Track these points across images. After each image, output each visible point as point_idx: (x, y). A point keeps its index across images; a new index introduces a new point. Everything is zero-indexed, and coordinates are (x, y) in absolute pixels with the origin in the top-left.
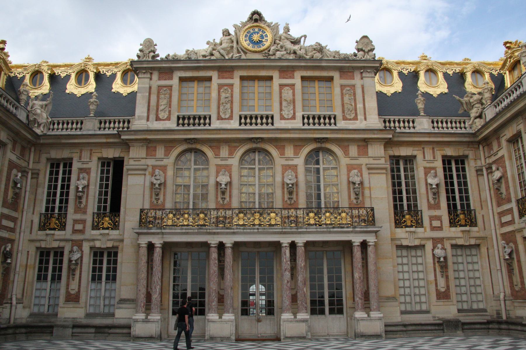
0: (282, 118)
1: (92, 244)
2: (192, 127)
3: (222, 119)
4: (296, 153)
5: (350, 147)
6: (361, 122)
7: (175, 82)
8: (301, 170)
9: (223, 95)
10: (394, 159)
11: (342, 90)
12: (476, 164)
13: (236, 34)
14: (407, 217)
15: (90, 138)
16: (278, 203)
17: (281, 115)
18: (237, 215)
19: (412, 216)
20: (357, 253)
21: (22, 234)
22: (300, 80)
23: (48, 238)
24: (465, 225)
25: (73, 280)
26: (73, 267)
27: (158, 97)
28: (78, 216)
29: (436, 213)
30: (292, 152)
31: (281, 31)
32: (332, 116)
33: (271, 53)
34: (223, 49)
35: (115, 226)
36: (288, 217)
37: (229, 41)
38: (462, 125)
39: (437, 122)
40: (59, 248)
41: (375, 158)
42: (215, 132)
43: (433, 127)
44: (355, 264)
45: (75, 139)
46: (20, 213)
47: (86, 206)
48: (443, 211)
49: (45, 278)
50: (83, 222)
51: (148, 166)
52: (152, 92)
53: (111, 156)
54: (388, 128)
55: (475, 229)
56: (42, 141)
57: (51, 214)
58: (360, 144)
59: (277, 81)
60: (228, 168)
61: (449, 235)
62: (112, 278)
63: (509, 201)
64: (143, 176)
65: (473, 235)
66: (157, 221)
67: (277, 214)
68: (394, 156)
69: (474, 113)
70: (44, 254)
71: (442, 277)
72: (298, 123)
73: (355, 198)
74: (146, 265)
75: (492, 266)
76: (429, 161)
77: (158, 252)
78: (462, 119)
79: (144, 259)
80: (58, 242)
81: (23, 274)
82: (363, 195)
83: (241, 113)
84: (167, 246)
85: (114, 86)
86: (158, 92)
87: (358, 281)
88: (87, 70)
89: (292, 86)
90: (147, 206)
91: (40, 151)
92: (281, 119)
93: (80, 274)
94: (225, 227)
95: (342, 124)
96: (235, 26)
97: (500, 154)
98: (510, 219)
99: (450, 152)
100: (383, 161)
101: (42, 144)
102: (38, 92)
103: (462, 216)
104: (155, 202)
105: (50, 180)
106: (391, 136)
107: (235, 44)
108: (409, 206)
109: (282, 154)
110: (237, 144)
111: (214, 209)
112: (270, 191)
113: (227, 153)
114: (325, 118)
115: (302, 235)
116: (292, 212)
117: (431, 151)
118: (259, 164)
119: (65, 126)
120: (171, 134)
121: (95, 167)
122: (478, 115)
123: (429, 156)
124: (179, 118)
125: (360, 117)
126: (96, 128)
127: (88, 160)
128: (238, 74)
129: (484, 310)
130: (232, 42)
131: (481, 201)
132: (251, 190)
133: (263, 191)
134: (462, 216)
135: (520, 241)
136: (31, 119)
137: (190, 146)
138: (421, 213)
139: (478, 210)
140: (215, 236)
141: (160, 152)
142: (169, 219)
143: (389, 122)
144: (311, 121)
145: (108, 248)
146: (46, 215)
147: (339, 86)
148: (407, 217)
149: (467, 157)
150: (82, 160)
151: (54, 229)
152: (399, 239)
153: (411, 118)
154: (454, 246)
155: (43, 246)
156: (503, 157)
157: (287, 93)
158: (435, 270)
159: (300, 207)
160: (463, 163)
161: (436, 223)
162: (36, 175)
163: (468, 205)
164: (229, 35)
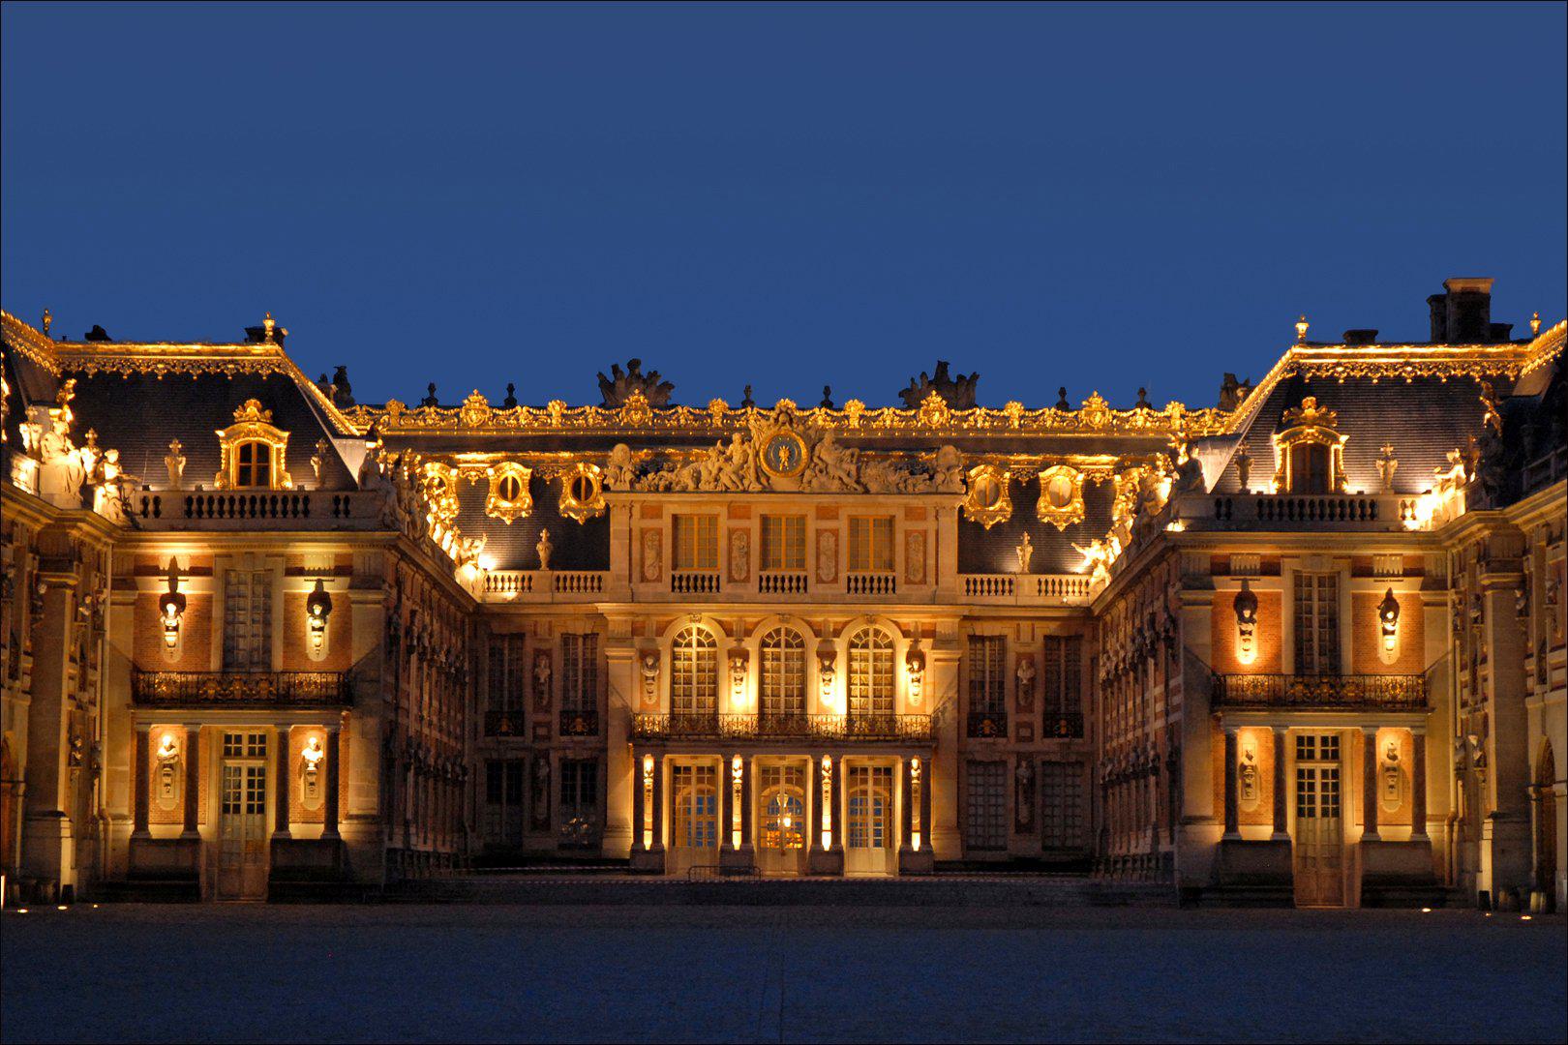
0: (820, 581)
1: (561, 754)
9: (736, 543)
27: (642, 544)
28: (541, 717)
29: (1025, 718)
47: (550, 703)
48: (1037, 720)
49: (499, 801)
50: (548, 725)
70: (493, 767)
125: (931, 579)
151: (507, 734)
154: (1044, 763)
155: (495, 756)
157: (828, 542)
162: (475, 661)
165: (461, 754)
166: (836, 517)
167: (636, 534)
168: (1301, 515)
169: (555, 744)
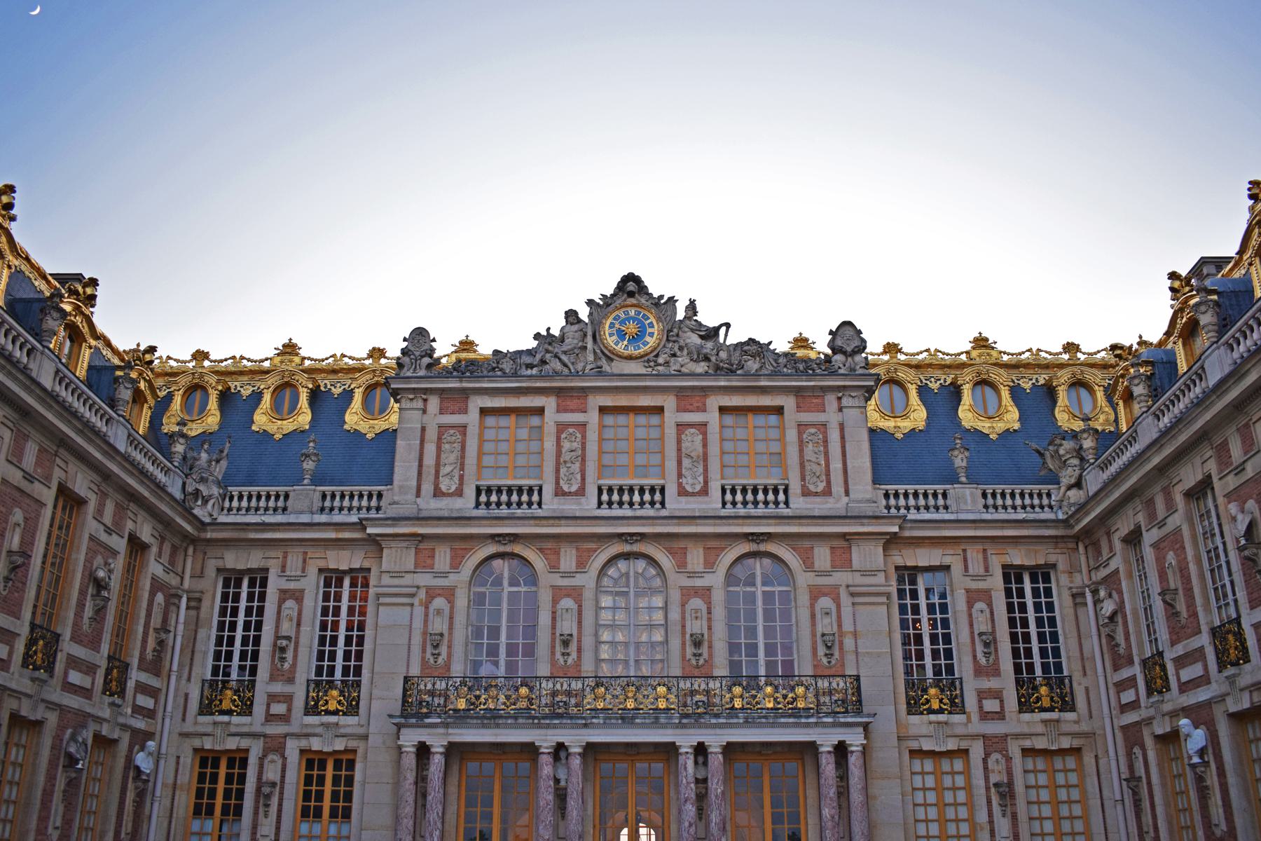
0: (682, 492)
1: (304, 743)
2: (504, 511)
3: (565, 494)
4: (710, 565)
5: (816, 550)
6: (838, 500)
7: (472, 418)
8: (718, 596)
9: (566, 445)
10: (906, 573)
11: (800, 434)
12: (1072, 582)
13: (592, 321)
14: (932, 691)
15: (305, 530)
17: (680, 485)
18: (593, 689)
19: (942, 691)
20: (828, 766)
21: (167, 721)
22: (717, 414)
23: (219, 731)
24: (1051, 709)
25: (266, 816)
26: (266, 790)
27: (439, 449)
28: (278, 688)
30: (702, 560)
31: (680, 315)
32: (781, 488)
33: (661, 360)
34: (565, 352)
36: (693, 693)
37: (579, 334)
38: (1045, 501)
39: (994, 495)
40: (238, 750)
41: (865, 573)
42: (551, 522)
43: (986, 507)
44: (824, 790)
45: (274, 531)
46: (166, 679)
47: (294, 665)
48: (1007, 681)
49: (210, 812)
50: (288, 699)
51: (418, 587)
52: (427, 437)
53: (344, 567)
54: (893, 511)
56: (209, 535)
57: (224, 682)
58: (836, 543)
60: (576, 593)
61: (1018, 730)
62: (342, 813)
63: (1131, 662)
64: (409, 608)
65: (1065, 728)
66: (436, 700)
67: (669, 689)
68: (906, 568)
69: (1068, 476)
70: (207, 760)
71: (1004, 816)
72: (713, 503)
73: (826, 655)
74: (413, 787)
75: (1105, 793)
77: (437, 761)
78: (1044, 488)
79: (411, 777)
80: (238, 738)
81: (167, 803)
82: (841, 649)
83: (601, 482)
84: (455, 751)
85: (348, 418)
86: (439, 439)
87: (830, 824)
88: (294, 382)
89: (702, 427)
90: (415, 671)
91: (205, 553)
92: (679, 495)
93: (280, 805)
95: (799, 504)
96: (590, 303)
97: (1113, 565)
98: (1133, 698)
99: (1018, 557)
100: (880, 579)
101: (209, 541)
102: (194, 430)
103: (1044, 690)
104: (432, 661)
105: (223, 612)
106: (896, 529)
108: (937, 671)
109: (681, 565)
110: (593, 546)
111: (548, 679)
112: (658, 636)
113: (574, 564)
114: (766, 491)
115: (718, 731)
116: (700, 684)
117: (980, 556)
118: (636, 586)
119: (254, 503)
120: (467, 525)
122: (1073, 481)
123: (976, 567)
124: (479, 491)
125: (837, 488)
126: (315, 509)
127: (299, 573)
130: (585, 335)
131: (1082, 659)
132: (620, 637)
133: (644, 638)
134: (1044, 690)
135: (1149, 742)
136: (190, 489)
137: (501, 549)
138: (961, 683)
139: (1077, 676)
140: (550, 732)
141: (443, 557)
142: (459, 696)
143: (896, 495)
144: (739, 497)
145: (336, 752)
146: (213, 684)
147: (794, 424)
148: (932, 691)
149: (1054, 566)
150: (288, 573)
151: (229, 712)
152: (916, 738)
153: (940, 488)
154: (1026, 752)
155: (208, 746)
156: (1117, 571)
157: (693, 441)
158: (989, 802)
159: (717, 673)
160: (1047, 579)
161: (991, 705)
162: (195, 603)
163: (1059, 667)
164: (580, 321)
167: (432, 434)
169: (294, 728)
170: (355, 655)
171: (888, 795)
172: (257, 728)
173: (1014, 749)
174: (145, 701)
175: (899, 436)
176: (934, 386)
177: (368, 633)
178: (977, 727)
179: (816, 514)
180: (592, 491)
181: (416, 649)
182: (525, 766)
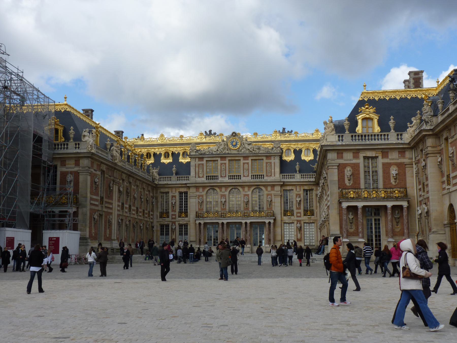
0: (244, 176)
1: (179, 222)
4: (249, 190)
8: (250, 196)
9: (222, 167)
16: (242, 209)
20: (267, 226)
28: (173, 213)
35: (187, 216)
41: (277, 191)
48: (302, 211)
50: (175, 215)
55: (313, 217)
59: (242, 161)
62: (186, 234)
65: (312, 219)
70: (162, 226)
72: (249, 179)
76: (298, 192)
84: (205, 224)
89: (248, 163)
94: (224, 217)
99: (306, 188)
107: (226, 146)
109: (244, 190)
112: (240, 203)
121: (177, 195)
123: (298, 189)
125: (273, 175)
128: (227, 159)
129: (314, 245)
132: (233, 203)
134: (309, 212)
141: (201, 190)
153: (293, 174)
154: (304, 223)
157: (246, 166)
161: (299, 215)
162: (157, 198)
165: (152, 223)
166: (248, 160)
167: (197, 165)
168: (365, 139)
170: (186, 206)
171: (278, 230)
172: (170, 220)
173: (302, 223)
174: (152, 217)
175: (288, 161)
176: (298, 149)
177: (188, 203)
178: (296, 218)
179: (269, 181)
180: (227, 176)
181: (197, 206)
182: (217, 226)
